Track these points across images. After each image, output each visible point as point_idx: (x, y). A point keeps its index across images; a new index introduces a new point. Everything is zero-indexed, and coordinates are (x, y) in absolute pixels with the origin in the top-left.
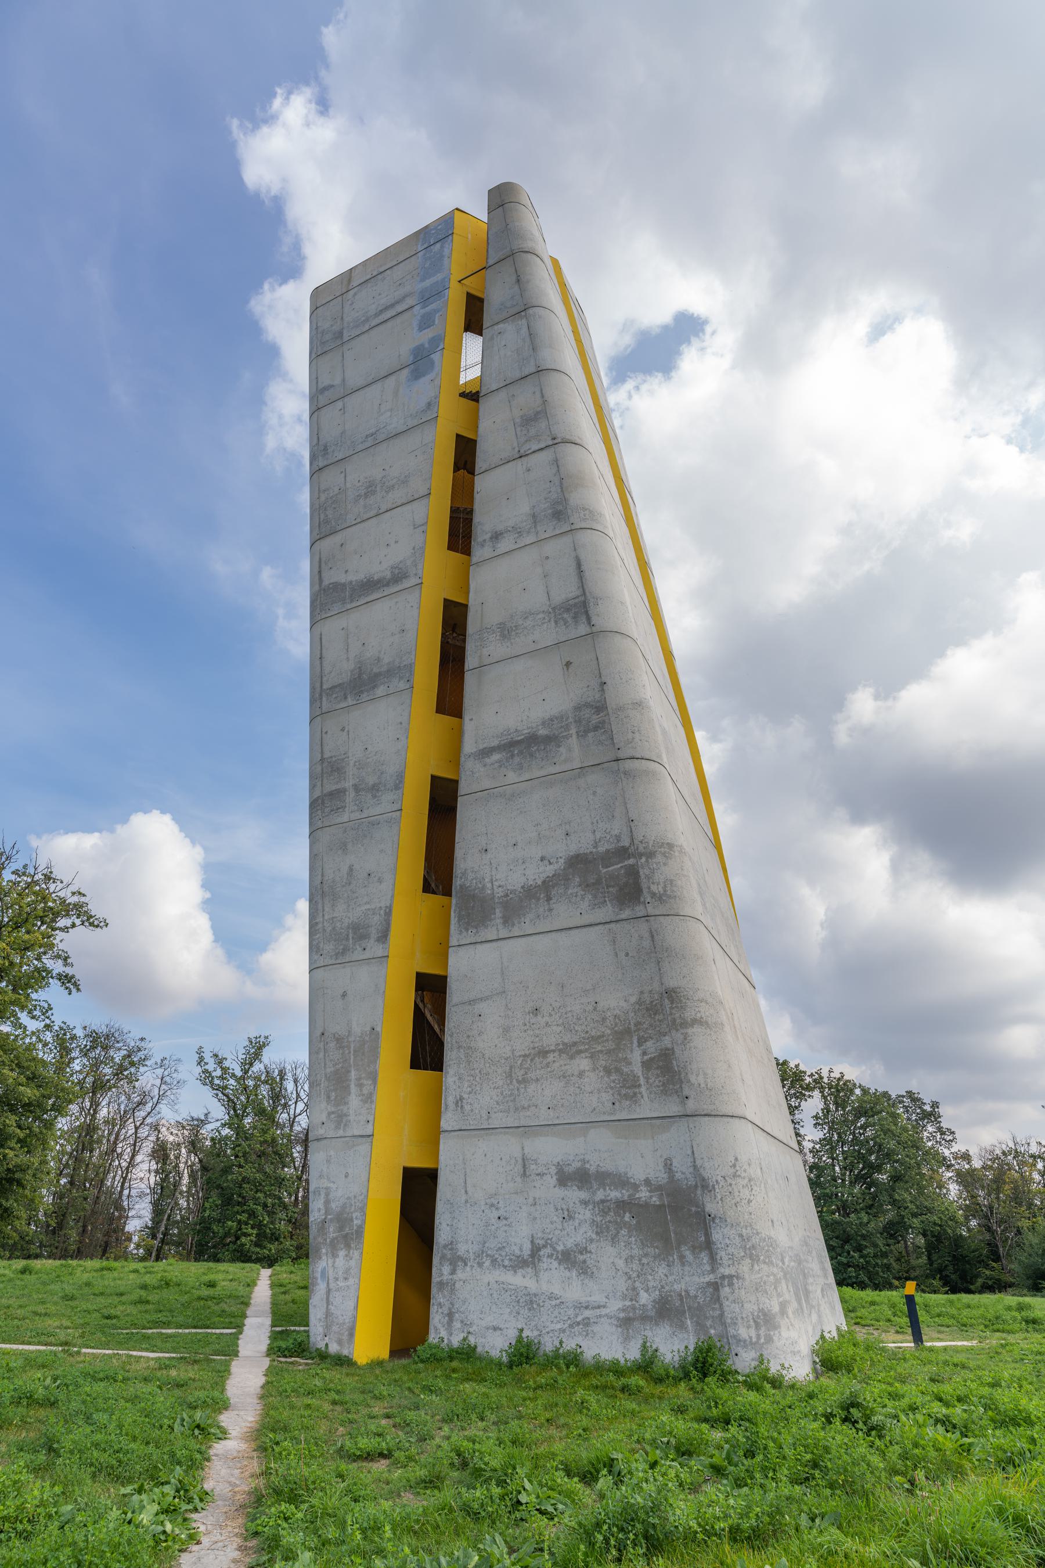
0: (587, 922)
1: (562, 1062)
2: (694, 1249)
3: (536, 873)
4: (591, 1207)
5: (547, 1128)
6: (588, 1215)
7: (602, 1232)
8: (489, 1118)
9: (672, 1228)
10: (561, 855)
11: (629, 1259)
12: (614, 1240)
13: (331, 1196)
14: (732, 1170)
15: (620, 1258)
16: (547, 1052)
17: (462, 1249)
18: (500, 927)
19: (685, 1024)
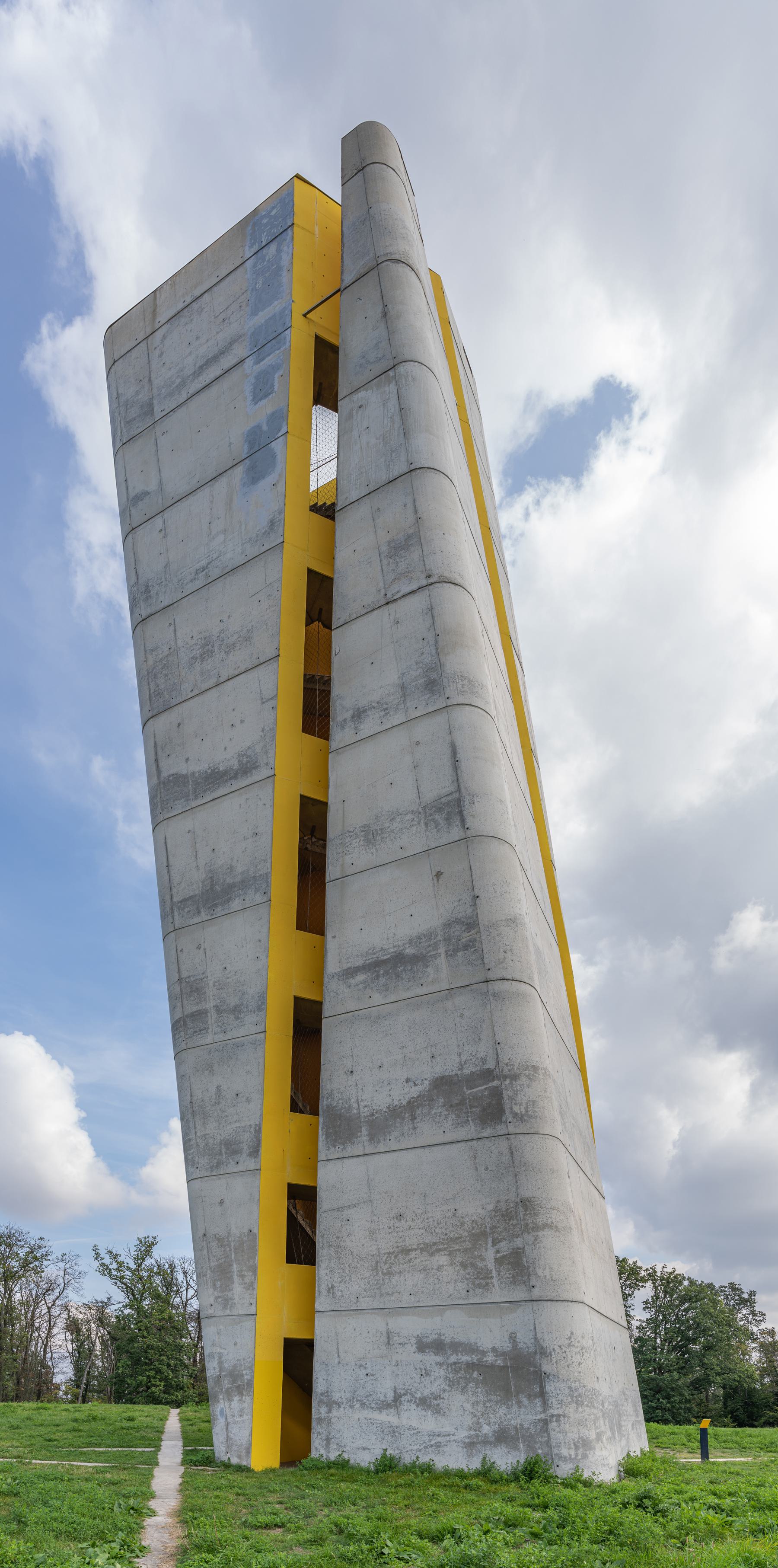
0: (450, 1140)
1: (423, 1259)
4: (445, 1367)
5: (409, 1309)
6: (442, 1372)
7: (454, 1385)
8: (357, 1302)
10: (426, 1077)
11: (475, 1404)
12: (463, 1390)
15: (468, 1402)
16: (410, 1250)
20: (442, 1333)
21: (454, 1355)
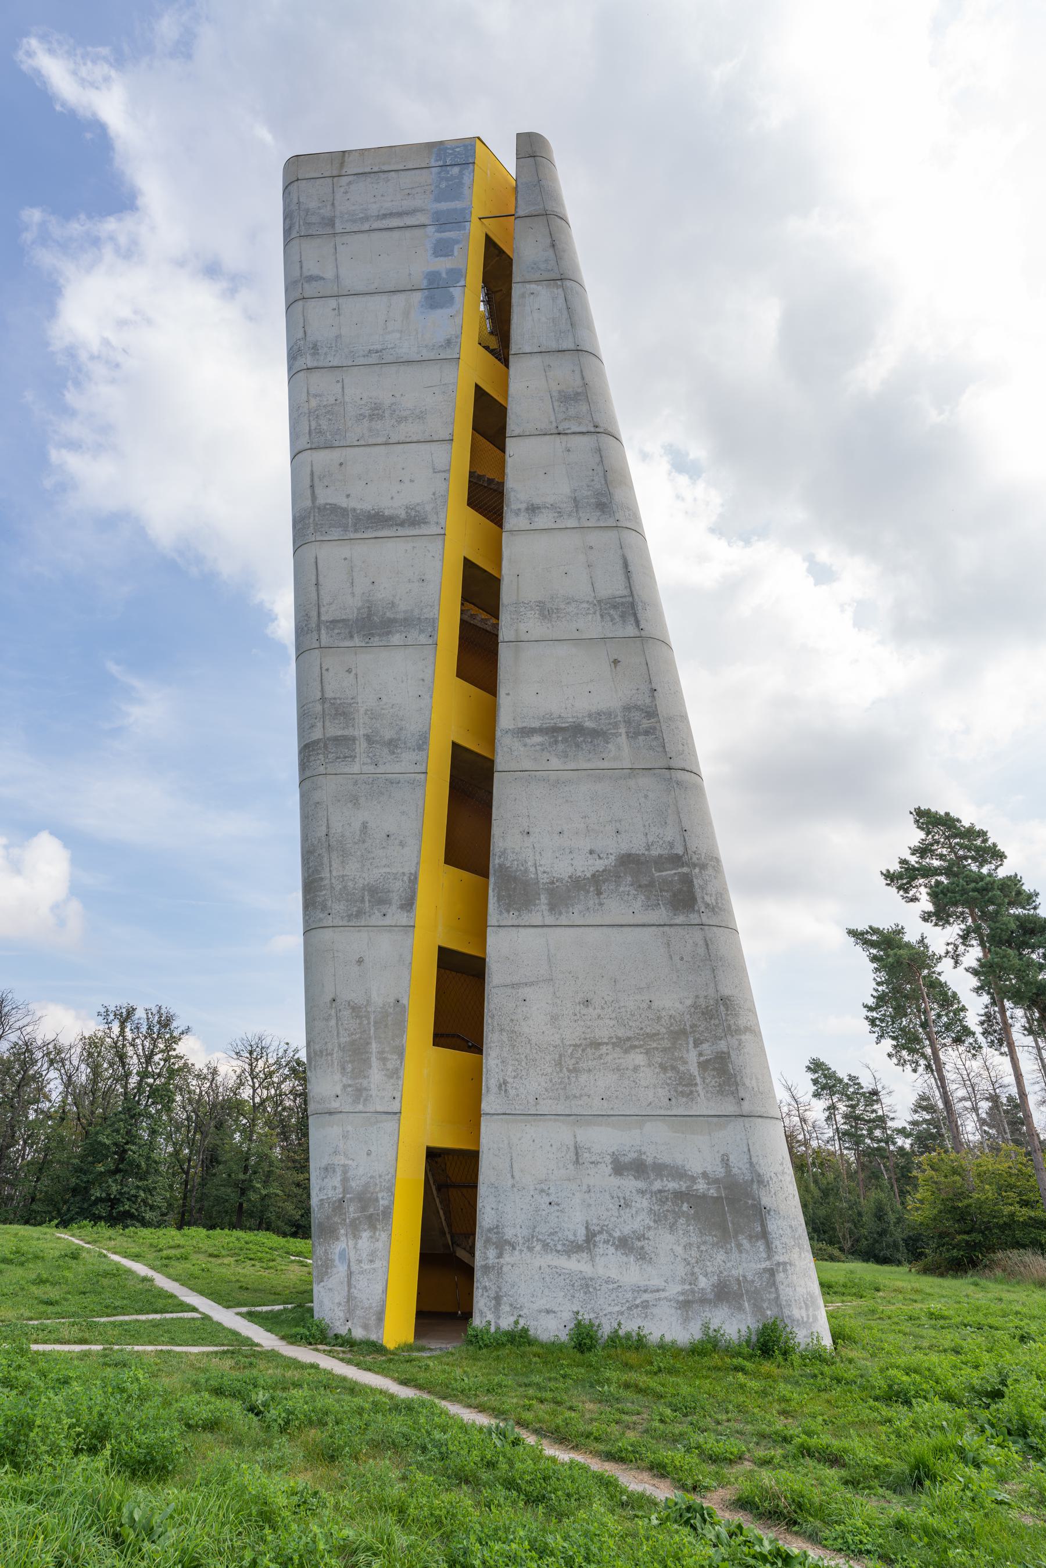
1: (616, 1056)
2: (750, 1238)
3: (585, 866)
4: (648, 1196)
5: (601, 1118)
6: (645, 1203)
7: (660, 1220)
8: (537, 1104)
9: (729, 1219)
11: (688, 1246)
12: (672, 1228)
13: (350, 1174)
14: (781, 1168)
15: (679, 1245)
16: (600, 1044)
17: (509, 1233)
18: (546, 913)
19: (738, 1031)
20: (643, 1150)
21: (659, 1181)
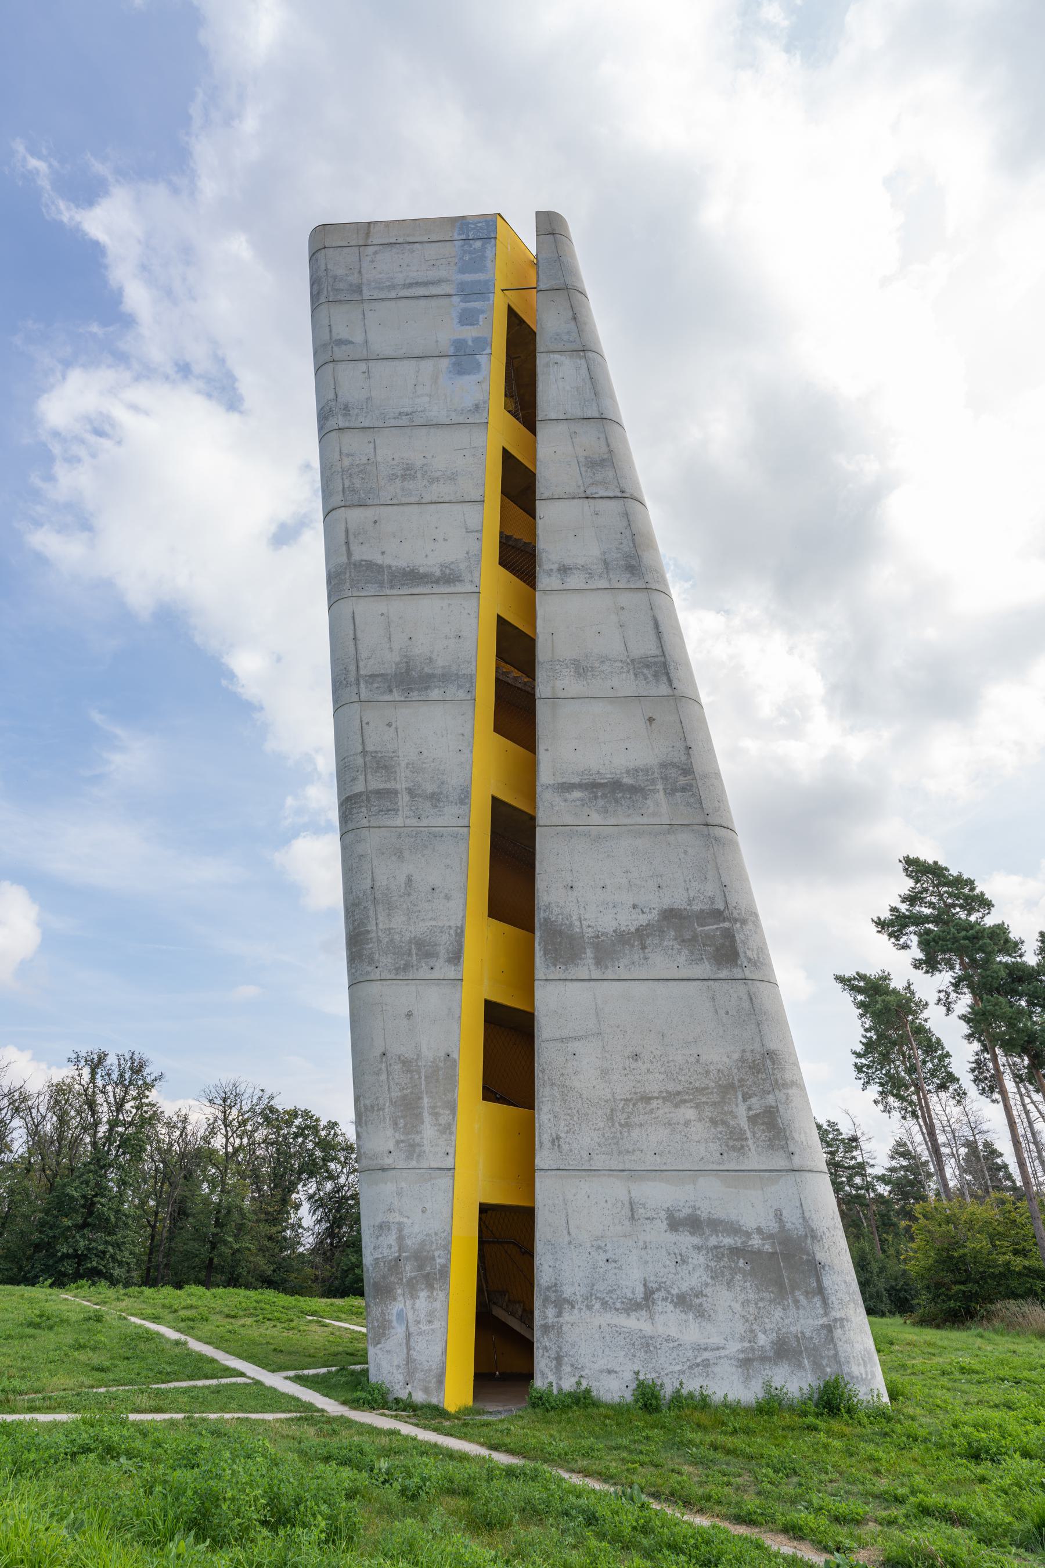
2: (807, 1293)
3: (629, 921)
4: (704, 1252)
5: (654, 1173)
6: (702, 1259)
7: (717, 1277)
8: (590, 1159)
9: (785, 1274)
10: (654, 906)
11: (746, 1303)
12: (730, 1284)
13: (406, 1232)
17: (568, 1292)
18: (592, 967)
19: (785, 1085)
20: (697, 1206)
21: (714, 1236)
